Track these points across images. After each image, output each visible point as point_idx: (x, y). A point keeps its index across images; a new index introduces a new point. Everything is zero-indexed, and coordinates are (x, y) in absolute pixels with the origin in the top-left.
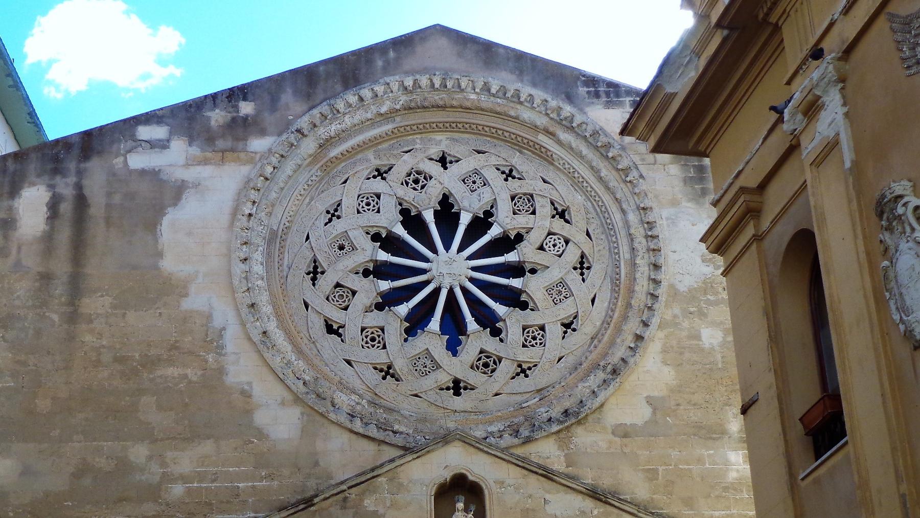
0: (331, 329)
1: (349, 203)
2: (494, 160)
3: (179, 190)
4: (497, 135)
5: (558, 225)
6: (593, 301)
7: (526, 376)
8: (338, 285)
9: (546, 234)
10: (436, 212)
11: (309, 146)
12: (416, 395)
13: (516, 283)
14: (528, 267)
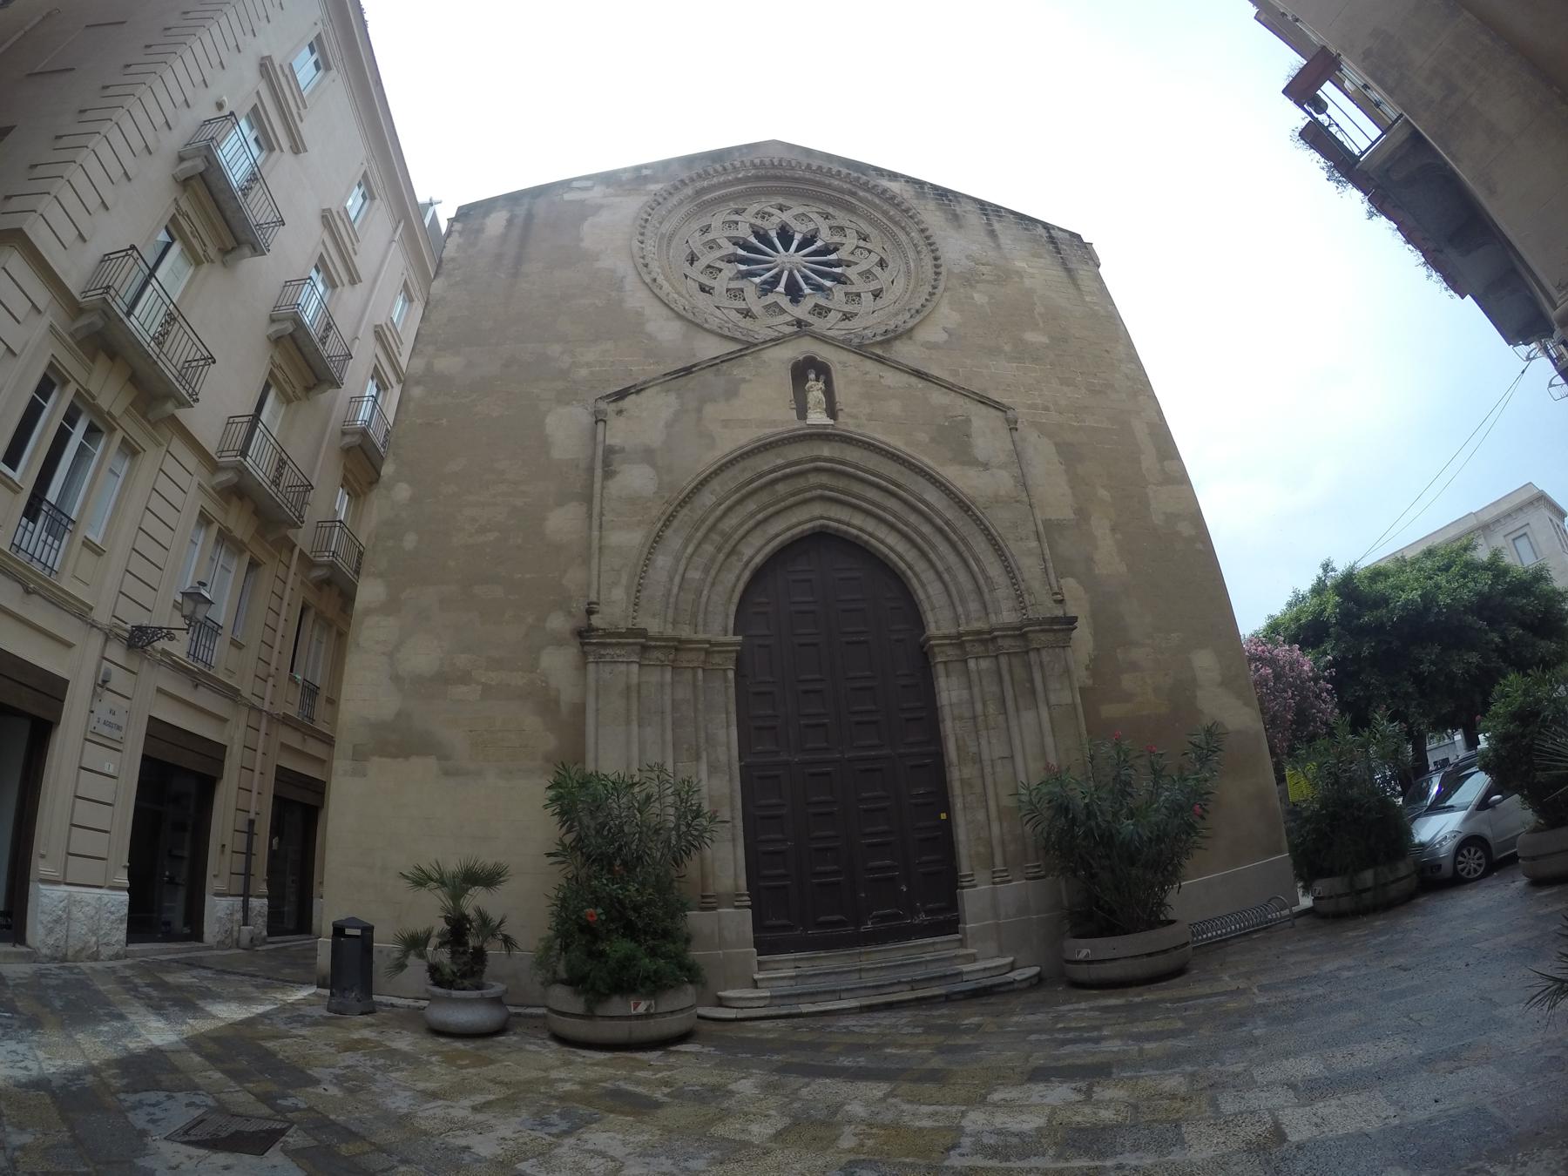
0: (703, 289)
1: (716, 222)
2: (815, 209)
3: (598, 208)
4: (817, 198)
5: (862, 243)
6: (893, 282)
7: (850, 320)
9: (854, 247)
10: (777, 233)
11: (689, 191)
12: (769, 327)
13: (838, 270)
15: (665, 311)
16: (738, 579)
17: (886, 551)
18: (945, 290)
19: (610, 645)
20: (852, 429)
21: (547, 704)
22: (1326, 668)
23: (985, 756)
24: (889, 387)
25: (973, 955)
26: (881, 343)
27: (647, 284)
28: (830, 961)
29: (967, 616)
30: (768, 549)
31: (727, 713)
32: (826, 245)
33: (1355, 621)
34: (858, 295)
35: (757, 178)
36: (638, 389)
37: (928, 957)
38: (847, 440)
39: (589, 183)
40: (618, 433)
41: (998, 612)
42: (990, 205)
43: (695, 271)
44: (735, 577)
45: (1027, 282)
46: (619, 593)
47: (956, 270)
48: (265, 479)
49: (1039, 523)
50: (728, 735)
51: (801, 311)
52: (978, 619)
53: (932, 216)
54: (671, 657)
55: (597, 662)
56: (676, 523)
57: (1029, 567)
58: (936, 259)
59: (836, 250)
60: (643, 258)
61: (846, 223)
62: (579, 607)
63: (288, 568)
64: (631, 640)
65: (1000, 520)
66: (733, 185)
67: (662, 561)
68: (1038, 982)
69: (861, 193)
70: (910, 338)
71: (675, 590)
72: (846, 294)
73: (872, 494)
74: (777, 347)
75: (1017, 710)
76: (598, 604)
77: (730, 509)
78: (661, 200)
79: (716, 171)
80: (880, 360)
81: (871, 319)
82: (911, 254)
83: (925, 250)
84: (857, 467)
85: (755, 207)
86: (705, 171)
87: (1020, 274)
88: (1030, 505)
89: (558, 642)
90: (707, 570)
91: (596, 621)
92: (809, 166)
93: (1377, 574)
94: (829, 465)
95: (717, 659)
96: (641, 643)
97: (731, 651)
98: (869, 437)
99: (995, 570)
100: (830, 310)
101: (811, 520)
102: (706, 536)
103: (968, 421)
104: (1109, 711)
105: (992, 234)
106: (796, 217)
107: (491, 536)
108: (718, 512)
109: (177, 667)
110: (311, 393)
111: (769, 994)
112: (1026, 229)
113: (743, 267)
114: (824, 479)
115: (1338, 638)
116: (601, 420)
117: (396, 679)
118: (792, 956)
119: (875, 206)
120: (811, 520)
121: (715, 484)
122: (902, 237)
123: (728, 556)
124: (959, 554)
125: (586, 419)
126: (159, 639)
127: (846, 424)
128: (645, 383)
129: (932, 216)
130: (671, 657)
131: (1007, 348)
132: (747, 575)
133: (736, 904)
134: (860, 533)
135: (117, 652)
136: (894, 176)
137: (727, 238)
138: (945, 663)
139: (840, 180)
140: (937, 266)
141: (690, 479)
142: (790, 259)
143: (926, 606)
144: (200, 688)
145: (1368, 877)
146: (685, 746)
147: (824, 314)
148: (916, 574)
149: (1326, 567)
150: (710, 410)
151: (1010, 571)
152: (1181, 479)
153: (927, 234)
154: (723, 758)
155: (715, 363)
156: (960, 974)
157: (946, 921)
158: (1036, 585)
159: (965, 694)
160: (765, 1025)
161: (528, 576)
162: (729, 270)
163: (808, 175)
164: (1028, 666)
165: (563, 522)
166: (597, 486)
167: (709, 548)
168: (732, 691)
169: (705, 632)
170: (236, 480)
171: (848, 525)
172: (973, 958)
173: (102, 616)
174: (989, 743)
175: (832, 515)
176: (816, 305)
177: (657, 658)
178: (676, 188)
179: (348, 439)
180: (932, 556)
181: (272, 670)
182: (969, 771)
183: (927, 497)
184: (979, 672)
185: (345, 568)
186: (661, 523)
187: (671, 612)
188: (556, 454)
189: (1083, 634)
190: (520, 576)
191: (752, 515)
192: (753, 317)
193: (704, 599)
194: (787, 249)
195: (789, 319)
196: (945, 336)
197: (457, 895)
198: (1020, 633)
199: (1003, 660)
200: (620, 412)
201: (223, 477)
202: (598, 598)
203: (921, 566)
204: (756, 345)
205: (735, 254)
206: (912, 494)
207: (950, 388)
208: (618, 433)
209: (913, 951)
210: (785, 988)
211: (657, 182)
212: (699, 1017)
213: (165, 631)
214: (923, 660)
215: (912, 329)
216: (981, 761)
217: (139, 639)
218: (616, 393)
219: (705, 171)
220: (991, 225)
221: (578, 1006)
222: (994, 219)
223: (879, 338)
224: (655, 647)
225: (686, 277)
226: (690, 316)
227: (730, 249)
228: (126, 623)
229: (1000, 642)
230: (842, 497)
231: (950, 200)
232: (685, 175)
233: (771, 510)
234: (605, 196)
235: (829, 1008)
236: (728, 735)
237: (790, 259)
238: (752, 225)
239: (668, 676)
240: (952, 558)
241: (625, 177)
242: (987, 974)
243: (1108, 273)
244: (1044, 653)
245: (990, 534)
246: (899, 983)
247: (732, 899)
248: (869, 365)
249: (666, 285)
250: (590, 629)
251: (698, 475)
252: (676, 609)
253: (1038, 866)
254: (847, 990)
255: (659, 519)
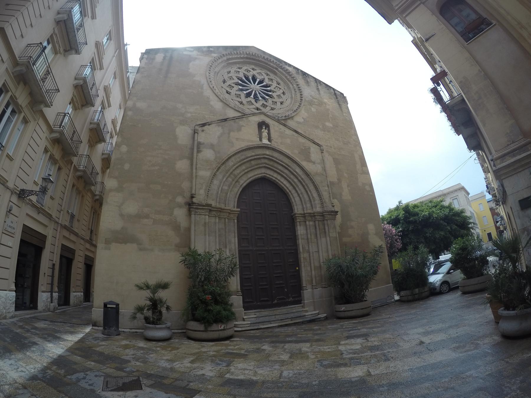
0: (227, 92)
1: (233, 71)
2: (264, 72)
5: (278, 86)
8: (229, 85)
11: (225, 58)
14: (272, 91)
15: (216, 98)
16: (238, 190)
17: (283, 186)
18: (304, 105)
19: (200, 209)
20: (276, 146)
21: (176, 227)
22: (399, 232)
23: (311, 251)
24: (287, 134)
25: (307, 310)
26: (284, 120)
27: (211, 88)
28: (265, 312)
29: (307, 208)
30: (248, 182)
31: (235, 233)
32: (267, 84)
33: (408, 219)
34: (276, 102)
35: (247, 58)
36: (209, 124)
37: (294, 311)
38: (274, 149)
39: (192, 50)
40: (202, 138)
41: (316, 208)
42: (318, 80)
43: (225, 86)
44: (237, 190)
45: (328, 107)
46: (202, 192)
47: (307, 100)
48: (69, 138)
49: (329, 182)
50: (235, 240)
51: (258, 105)
52: (310, 209)
53: (301, 81)
54: (218, 214)
55: (195, 214)
56: (220, 170)
57: (325, 195)
58: (301, 95)
59: (269, 86)
60: (210, 79)
61: (274, 78)
62: (187, 195)
63: (70, 171)
64: (207, 208)
65: (318, 180)
66: (239, 59)
67: (216, 182)
68: (326, 318)
69: (279, 69)
70: (293, 119)
71: (220, 192)
72: (272, 101)
73: (280, 167)
74: (254, 117)
75: (320, 237)
76: (195, 195)
77: (237, 167)
78: (216, 60)
79: (234, 53)
80: (285, 125)
81: (280, 111)
82: (293, 92)
83: (298, 91)
84: (276, 158)
85: (245, 68)
86: (231, 53)
87: (325, 103)
88: (326, 176)
89: (180, 206)
90: (229, 186)
91: (194, 200)
92: (264, 57)
93: (415, 206)
94: (268, 157)
95: (232, 216)
96: (209, 209)
97: (236, 214)
98: (281, 150)
99: (315, 195)
100: (267, 106)
101: (261, 174)
102: (229, 175)
103: (309, 148)
104: (345, 240)
105: (318, 89)
106: (258, 73)
107: (157, 168)
108: (234, 168)
109: (33, 206)
110: (83, 107)
111: (250, 323)
112: (328, 90)
113: (241, 87)
114: (266, 161)
115: (403, 224)
116: (197, 133)
117: (122, 215)
118: (254, 311)
119: (283, 74)
120: (261, 174)
121: (233, 159)
122: (291, 86)
123: (236, 182)
124: (305, 189)
125: (190, 131)
126: (32, 195)
127: (274, 144)
128: (211, 122)
129: (301, 81)
130: (218, 214)
131: (321, 127)
132: (241, 189)
133: (238, 294)
134: (276, 179)
135: (15, 199)
136: (290, 65)
137: (236, 76)
138: (299, 222)
139: (273, 64)
140: (301, 97)
141: (225, 156)
142: (255, 87)
143: (294, 204)
144: (40, 214)
145: (417, 291)
146: (222, 243)
147: (265, 107)
148: (292, 194)
149: (400, 202)
150: (232, 134)
151: (320, 195)
152: (367, 173)
153: (299, 86)
154: (233, 248)
155: (234, 119)
156: (305, 315)
157: (298, 301)
158: (327, 201)
159: (305, 231)
160: (252, 332)
161: (169, 183)
162: (236, 87)
163: (263, 60)
164: (324, 225)
165: (182, 165)
166: (195, 154)
167: (230, 179)
168: (236, 226)
169: (228, 207)
170: (59, 137)
171: (272, 176)
172: (307, 311)
173: (10, 185)
174: (312, 247)
175: (268, 173)
176: (263, 104)
177: (214, 214)
178: (221, 57)
179: (92, 126)
180: (297, 189)
181: (63, 208)
182: (306, 255)
183: (297, 170)
184: (309, 225)
185: (88, 173)
186: (216, 170)
187: (218, 199)
188: (179, 142)
189: (339, 217)
190: (166, 182)
191: (244, 170)
192: (243, 105)
193: (228, 196)
194: (254, 84)
195: (255, 107)
196: (303, 120)
197: (154, 291)
198: (322, 214)
199: (317, 222)
200: (203, 131)
201: (55, 135)
202: (195, 192)
203: (293, 191)
204: (247, 115)
205: (238, 82)
206: (292, 169)
207: (305, 137)
208: (202, 138)
209: (289, 309)
210: (254, 320)
211: (215, 53)
212: (235, 331)
213: (34, 192)
214: (292, 220)
215: (293, 117)
216: (309, 252)
217: (22, 194)
218: (202, 124)
219: (231, 53)
220: (318, 86)
221: (201, 327)
222: (319, 85)
223: (284, 118)
224: (214, 210)
225: (222, 87)
226: (225, 101)
227: (237, 80)
228: (18, 188)
229: (316, 217)
230: (271, 167)
231: (306, 76)
232: (224, 53)
233: (250, 169)
234: (197, 55)
235: (269, 326)
236: (235, 240)
237: (255, 87)
238: (244, 74)
239: (217, 220)
240: (303, 190)
241: (205, 49)
242: (312, 316)
243: (352, 107)
244: (328, 221)
245: (314, 184)
246: (288, 318)
247: (236, 293)
248: (281, 127)
249: (217, 90)
250: (193, 203)
251: (228, 155)
252: (220, 198)
253: (325, 284)
254: (273, 321)
255: (215, 168)
